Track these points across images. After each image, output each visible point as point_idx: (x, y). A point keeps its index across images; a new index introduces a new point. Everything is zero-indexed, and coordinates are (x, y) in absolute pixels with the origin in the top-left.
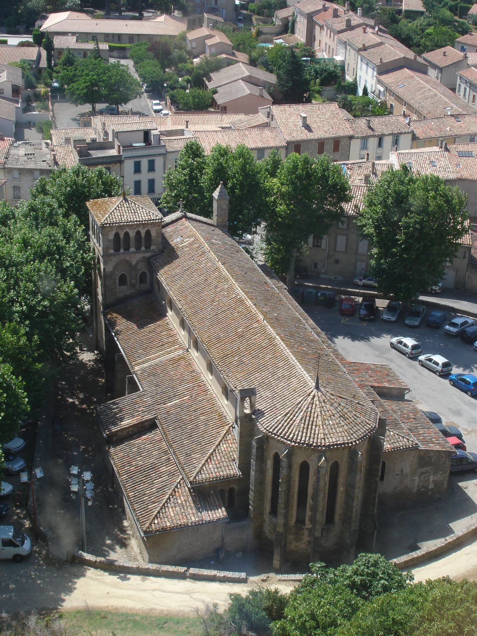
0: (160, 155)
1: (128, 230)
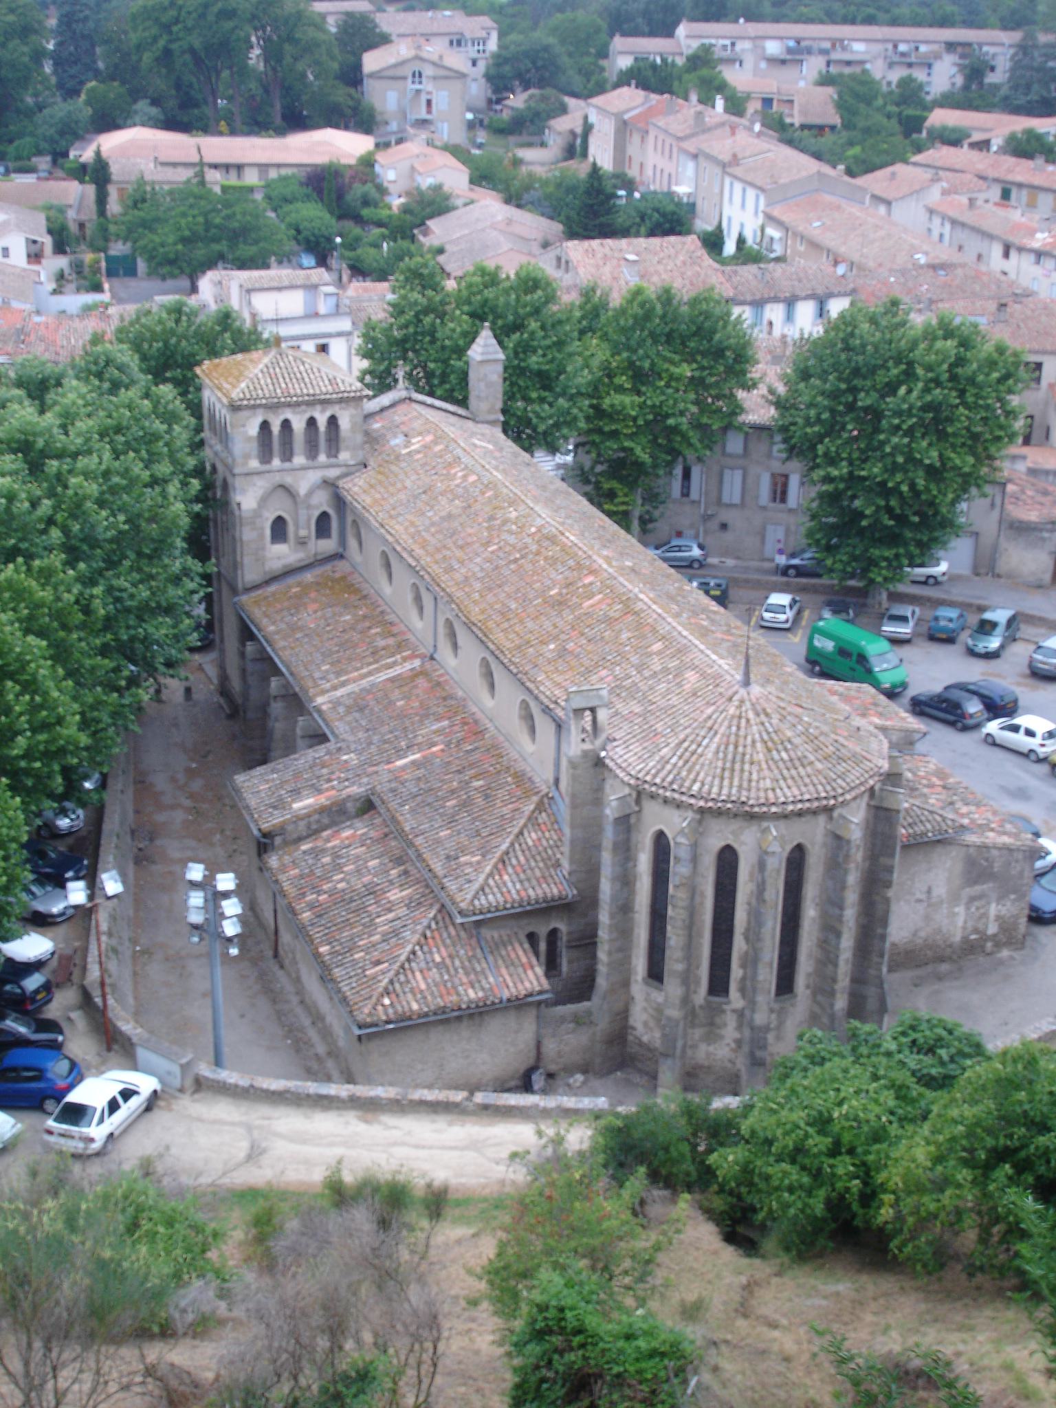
0: (340, 334)
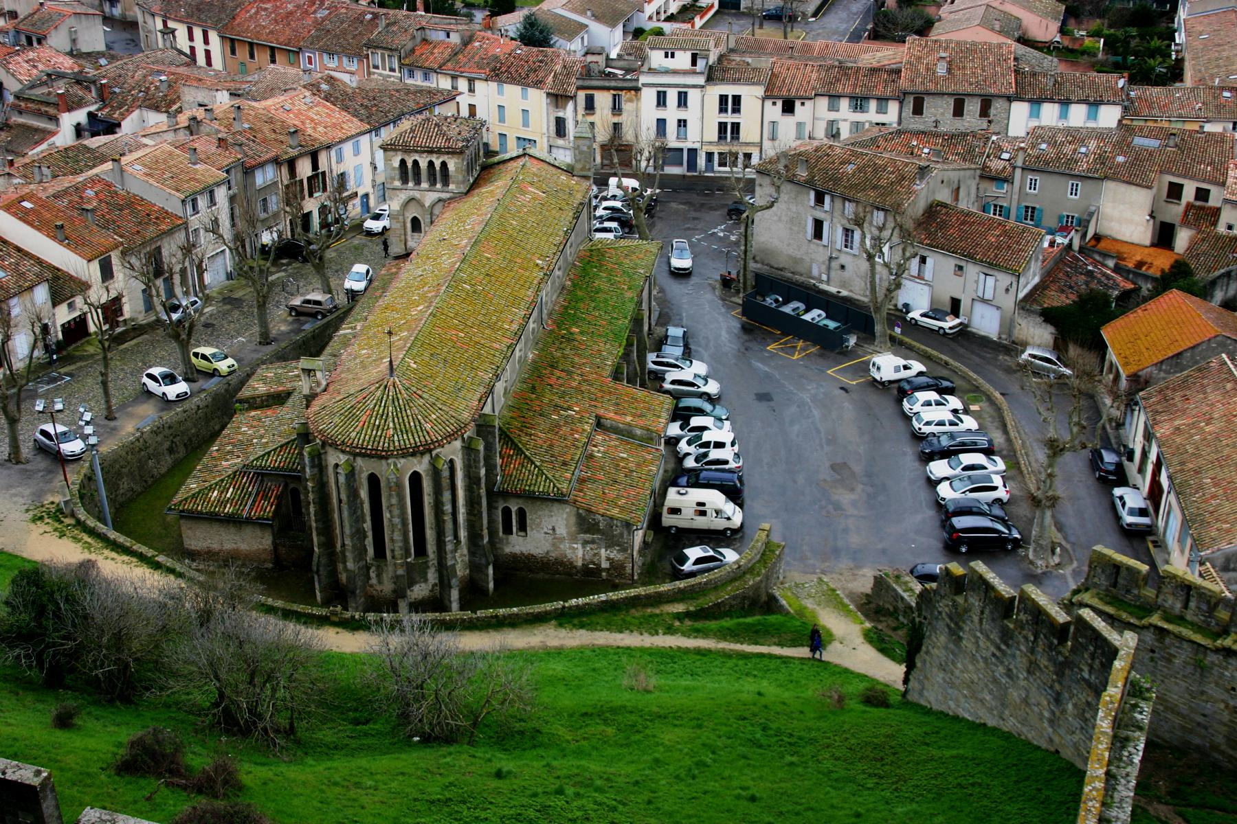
0: (694, 86)
1: (417, 158)
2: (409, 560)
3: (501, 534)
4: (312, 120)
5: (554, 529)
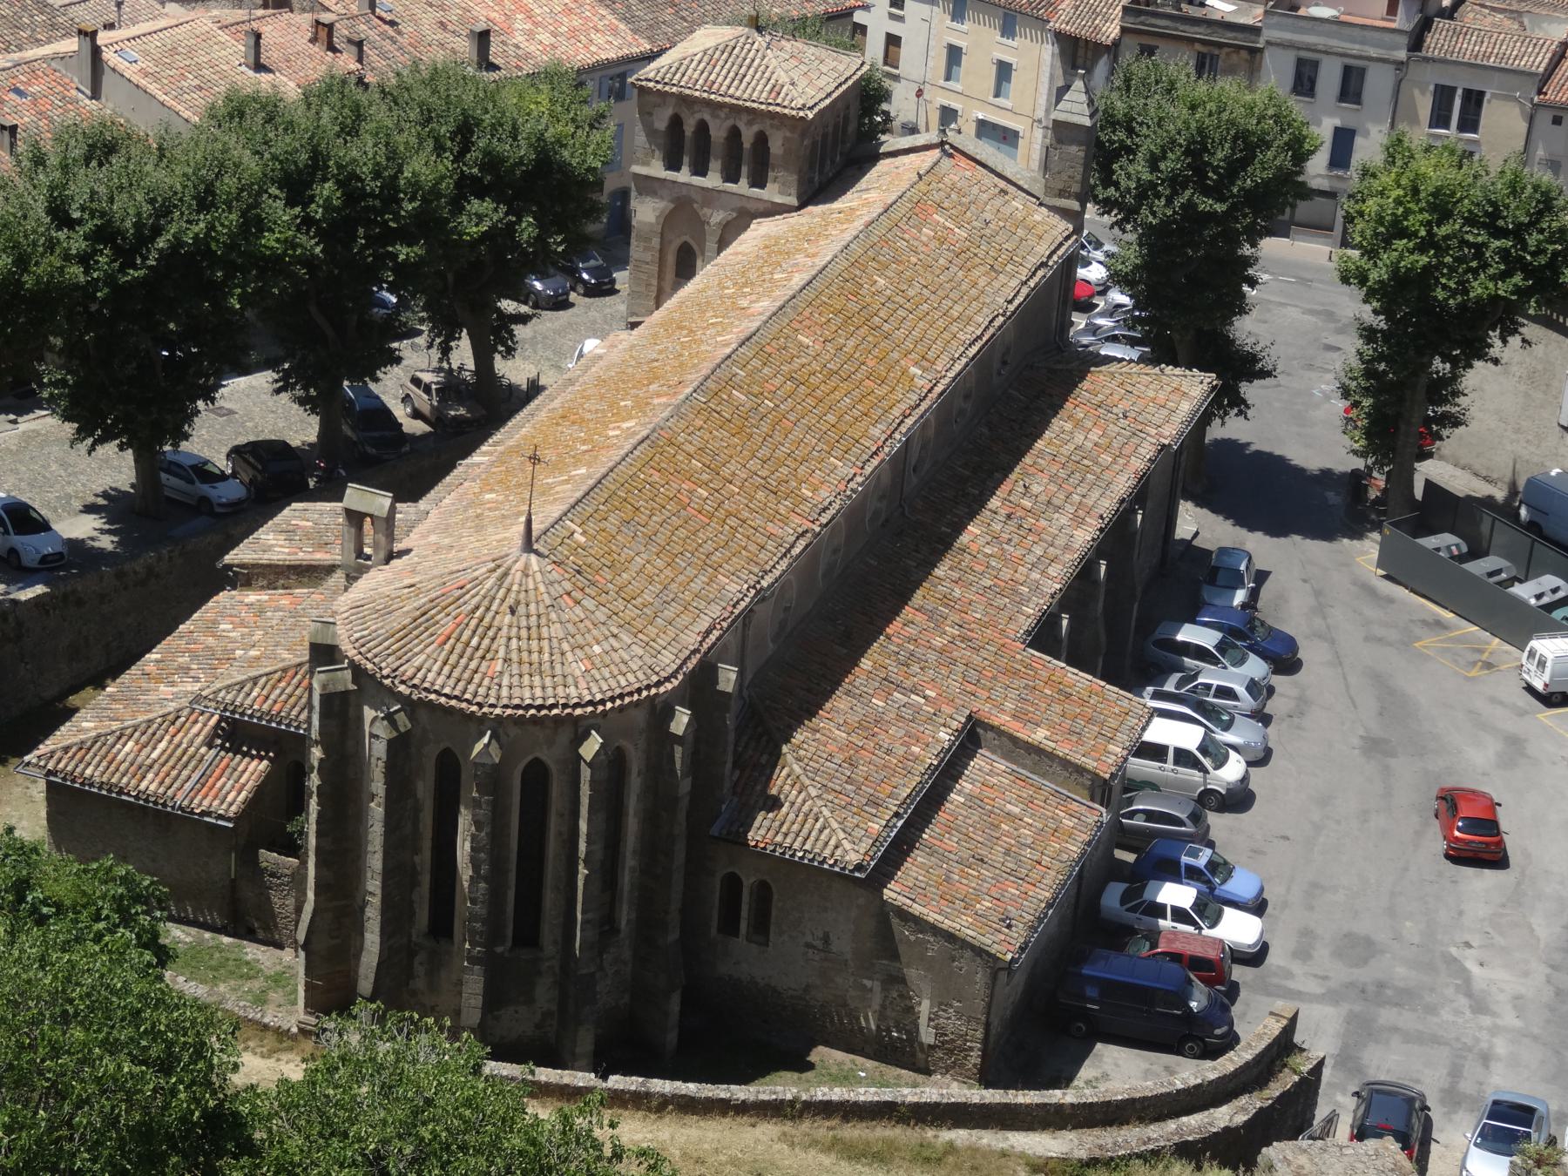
1: (707, 117)
2: (499, 949)
3: (714, 931)
4: (530, 16)
5: (826, 939)
